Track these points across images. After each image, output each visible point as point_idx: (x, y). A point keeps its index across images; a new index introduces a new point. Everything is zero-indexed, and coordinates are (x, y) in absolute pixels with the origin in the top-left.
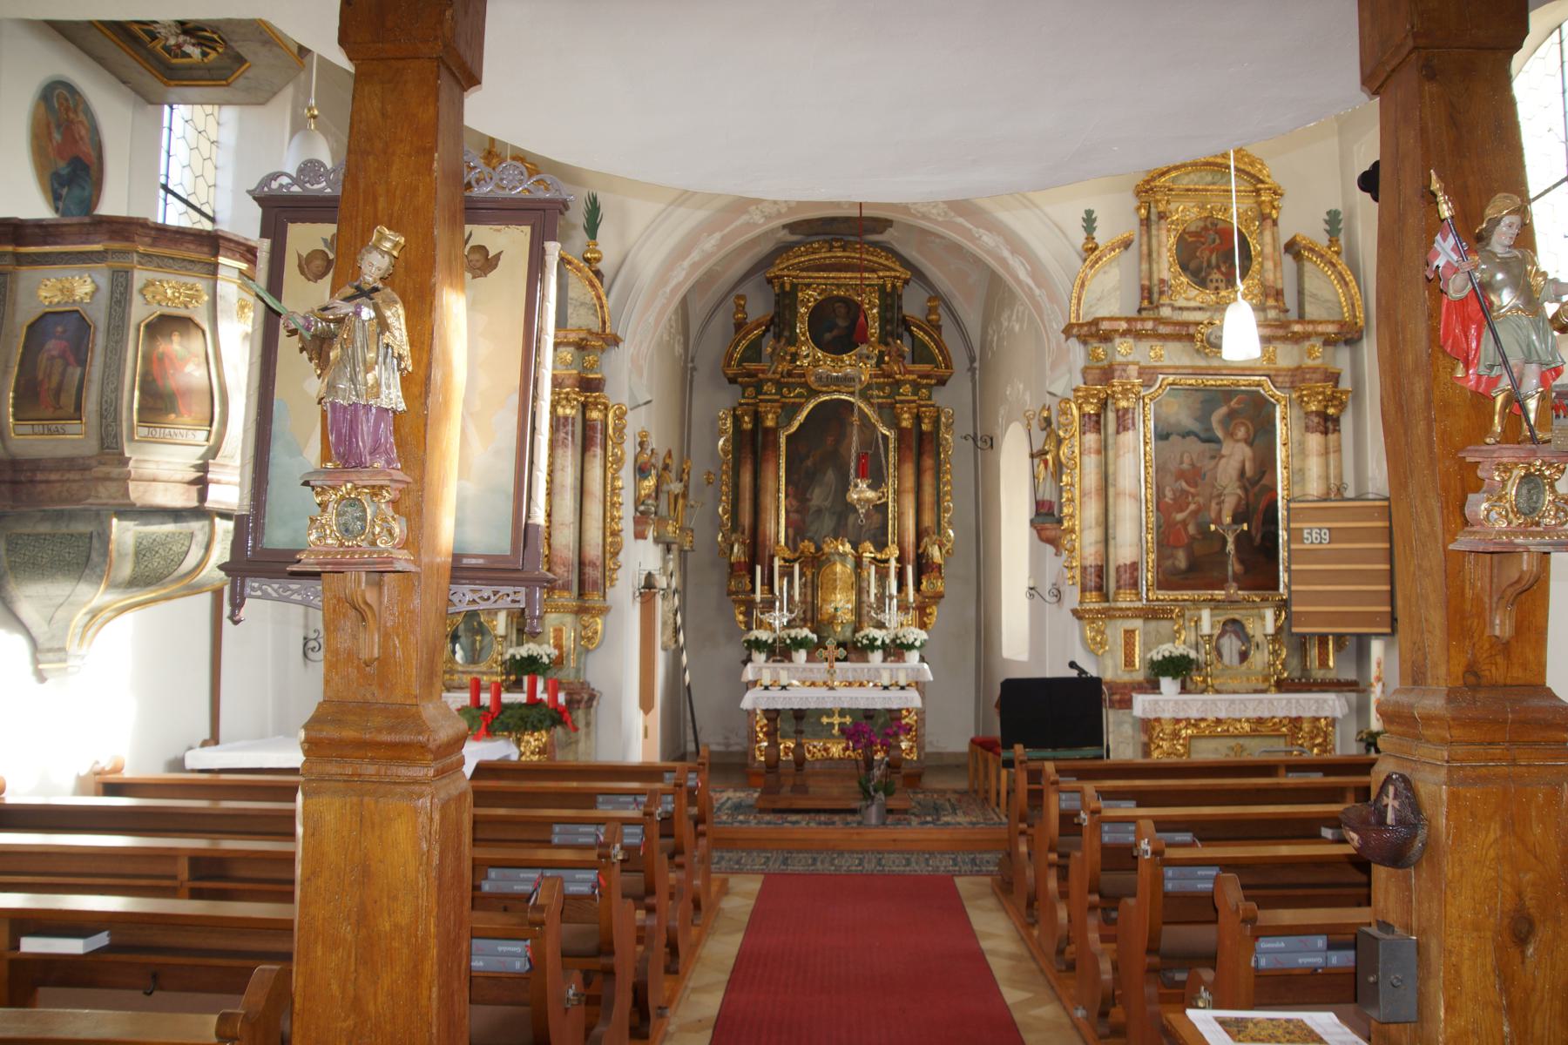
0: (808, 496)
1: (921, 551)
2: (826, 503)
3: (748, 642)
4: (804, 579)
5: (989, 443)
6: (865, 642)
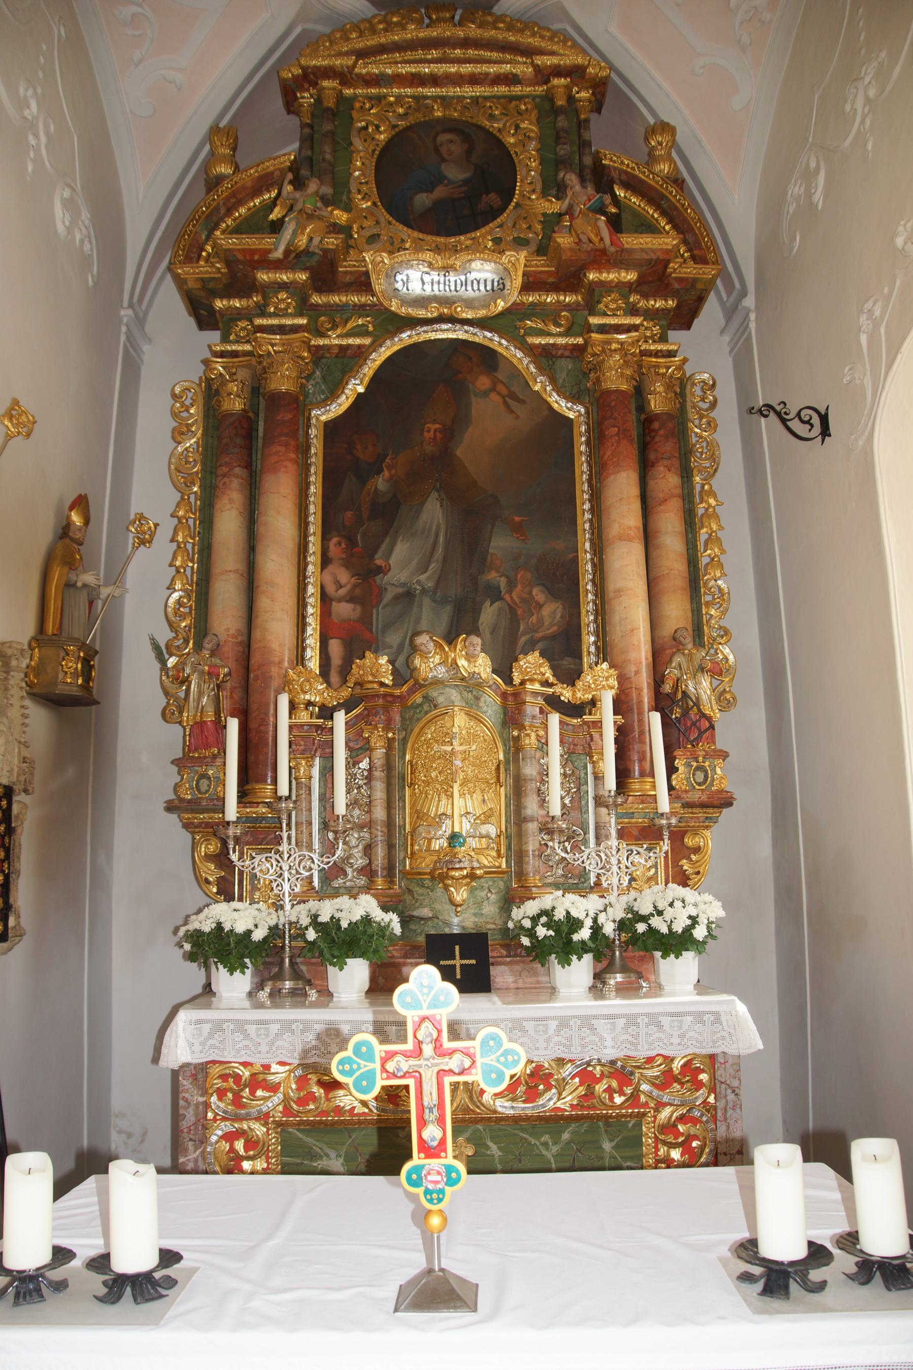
1: (667, 688)
2: (423, 577)
3: (196, 937)
4: (364, 765)
5: (816, 420)
6: (541, 932)
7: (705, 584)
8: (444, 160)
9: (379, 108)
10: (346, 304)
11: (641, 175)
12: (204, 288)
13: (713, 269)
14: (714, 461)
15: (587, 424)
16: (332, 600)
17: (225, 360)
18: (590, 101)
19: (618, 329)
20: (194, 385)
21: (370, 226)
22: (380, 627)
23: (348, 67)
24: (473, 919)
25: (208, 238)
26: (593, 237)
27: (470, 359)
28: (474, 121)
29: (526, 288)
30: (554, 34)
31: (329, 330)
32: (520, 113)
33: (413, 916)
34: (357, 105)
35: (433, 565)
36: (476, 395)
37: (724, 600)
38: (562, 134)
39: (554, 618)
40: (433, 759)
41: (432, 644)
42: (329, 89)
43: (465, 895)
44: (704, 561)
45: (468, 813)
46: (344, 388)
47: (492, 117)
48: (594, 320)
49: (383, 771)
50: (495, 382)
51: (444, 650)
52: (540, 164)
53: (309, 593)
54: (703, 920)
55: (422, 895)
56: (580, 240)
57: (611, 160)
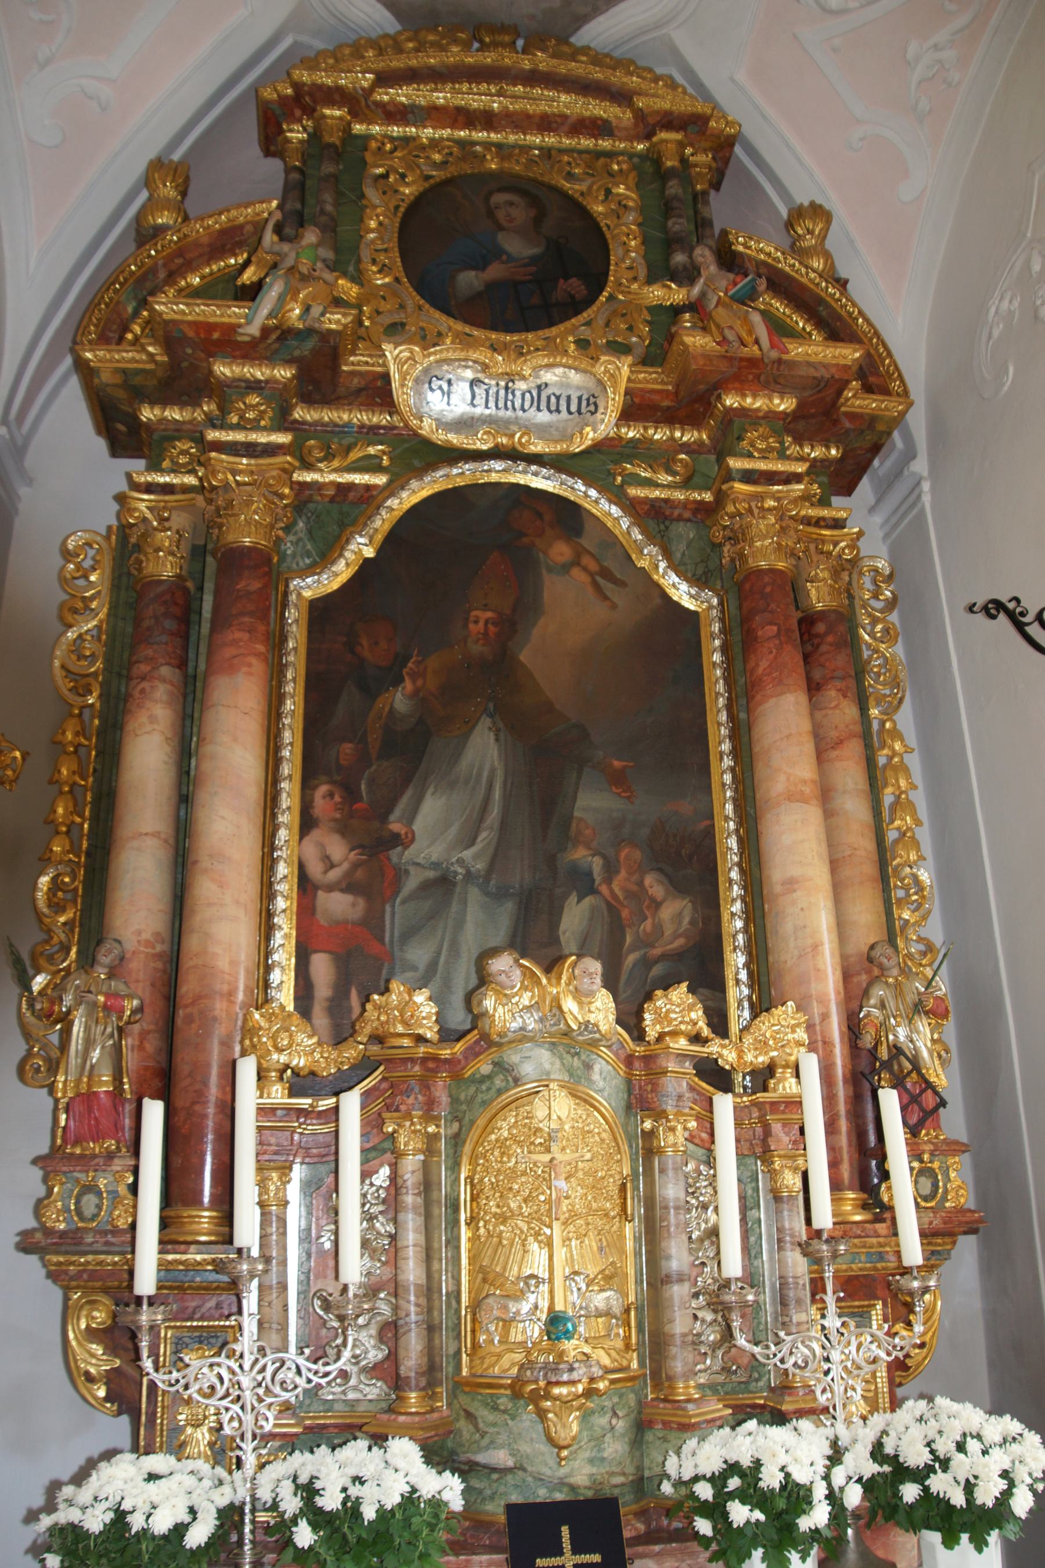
2: (467, 854)
7: (896, 870)
8: (501, 228)
9: (406, 152)
10: (348, 424)
11: (787, 269)
12: (126, 385)
13: (900, 404)
14: (898, 686)
15: (722, 620)
16: (316, 888)
17: (152, 497)
18: (710, 168)
19: (771, 478)
20: (99, 539)
21: (390, 312)
22: (396, 934)
23: (363, 89)
24: (588, 1470)
25: (136, 313)
26: (744, 335)
27: (540, 515)
28: (546, 179)
29: (628, 414)
30: (656, 79)
31: (321, 461)
32: (611, 174)
33: (477, 1464)
34: (374, 145)
35: (484, 834)
36: (550, 570)
37: (923, 897)
38: (675, 204)
39: (680, 923)
40: (513, 1174)
41: (518, 972)
42: (332, 117)
43: (575, 1427)
44: (892, 835)
45: (576, 1273)
46: (343, 549)
47: (570, 176)
48: (735, 463)
49: (419, 1194)
50: (579, 553)
51: (539, 982)
52: (643, 243)
53: (279, 876)
55: (495, 1425)
56: (724, 338)
57: (745, 245)
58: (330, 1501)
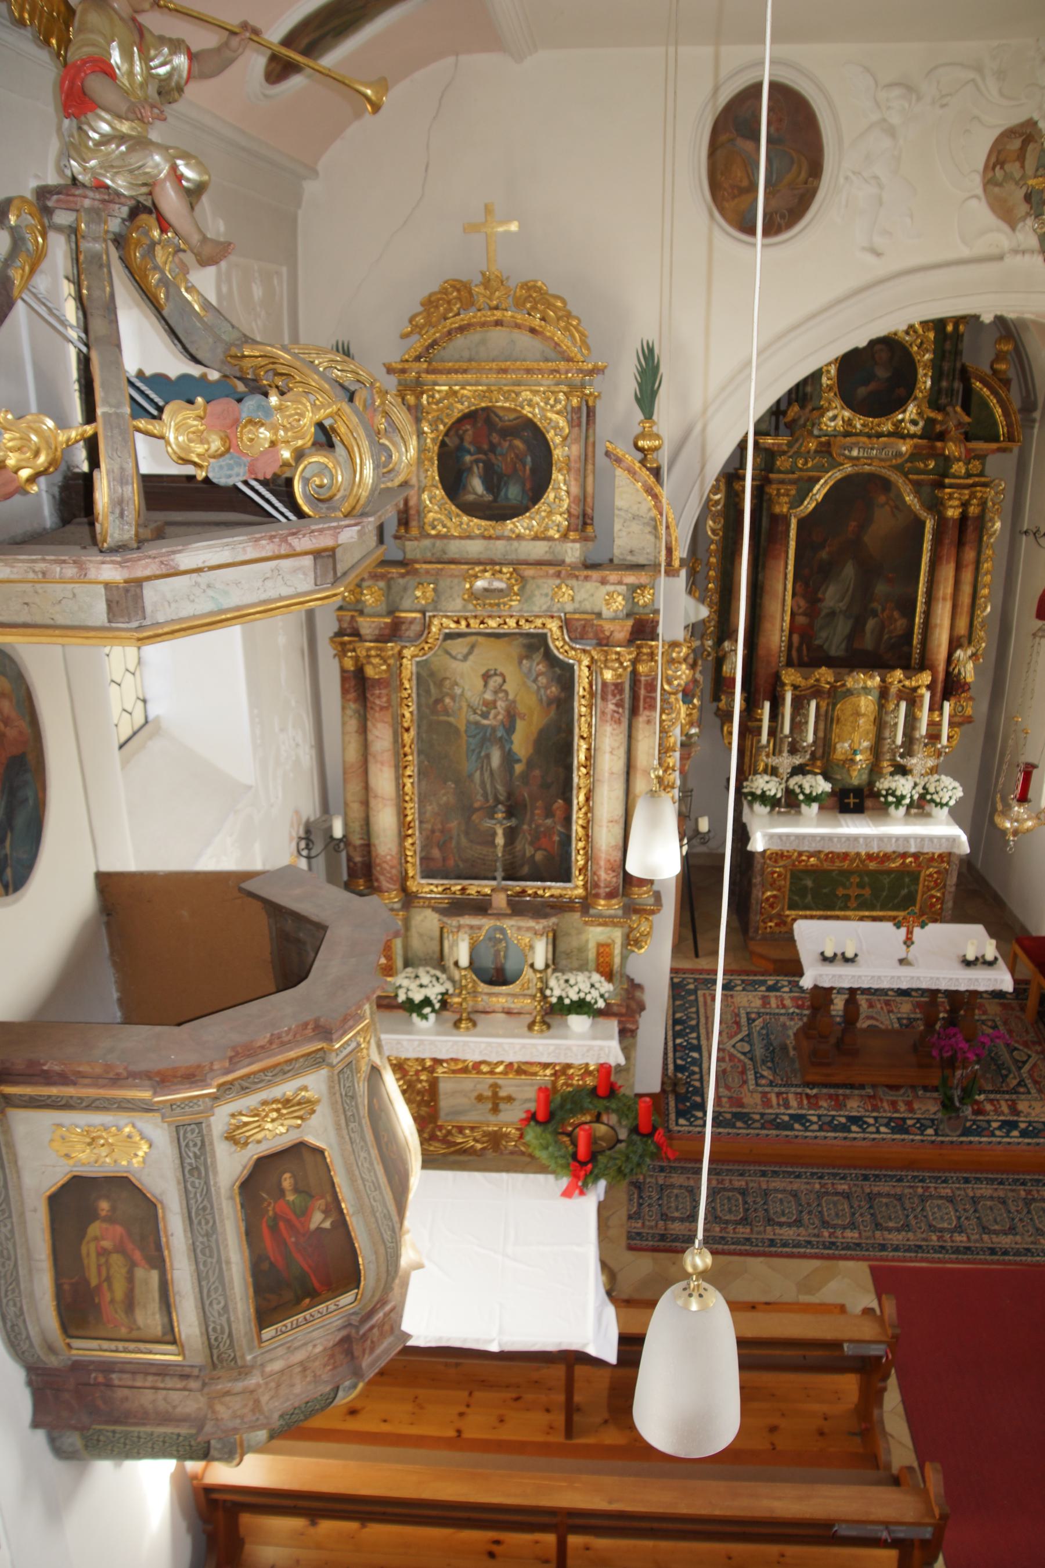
0: (820, 595)
2: (841, 604)
54: (954, 798)
58: (807, 791)
